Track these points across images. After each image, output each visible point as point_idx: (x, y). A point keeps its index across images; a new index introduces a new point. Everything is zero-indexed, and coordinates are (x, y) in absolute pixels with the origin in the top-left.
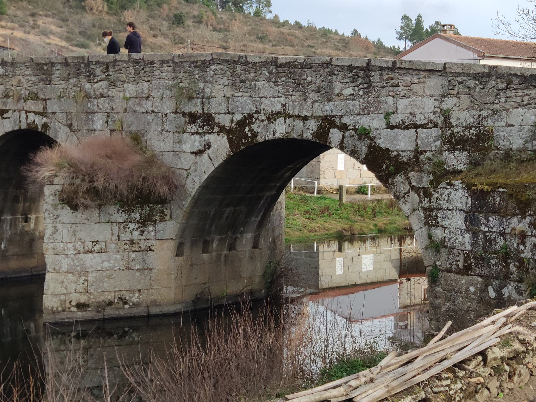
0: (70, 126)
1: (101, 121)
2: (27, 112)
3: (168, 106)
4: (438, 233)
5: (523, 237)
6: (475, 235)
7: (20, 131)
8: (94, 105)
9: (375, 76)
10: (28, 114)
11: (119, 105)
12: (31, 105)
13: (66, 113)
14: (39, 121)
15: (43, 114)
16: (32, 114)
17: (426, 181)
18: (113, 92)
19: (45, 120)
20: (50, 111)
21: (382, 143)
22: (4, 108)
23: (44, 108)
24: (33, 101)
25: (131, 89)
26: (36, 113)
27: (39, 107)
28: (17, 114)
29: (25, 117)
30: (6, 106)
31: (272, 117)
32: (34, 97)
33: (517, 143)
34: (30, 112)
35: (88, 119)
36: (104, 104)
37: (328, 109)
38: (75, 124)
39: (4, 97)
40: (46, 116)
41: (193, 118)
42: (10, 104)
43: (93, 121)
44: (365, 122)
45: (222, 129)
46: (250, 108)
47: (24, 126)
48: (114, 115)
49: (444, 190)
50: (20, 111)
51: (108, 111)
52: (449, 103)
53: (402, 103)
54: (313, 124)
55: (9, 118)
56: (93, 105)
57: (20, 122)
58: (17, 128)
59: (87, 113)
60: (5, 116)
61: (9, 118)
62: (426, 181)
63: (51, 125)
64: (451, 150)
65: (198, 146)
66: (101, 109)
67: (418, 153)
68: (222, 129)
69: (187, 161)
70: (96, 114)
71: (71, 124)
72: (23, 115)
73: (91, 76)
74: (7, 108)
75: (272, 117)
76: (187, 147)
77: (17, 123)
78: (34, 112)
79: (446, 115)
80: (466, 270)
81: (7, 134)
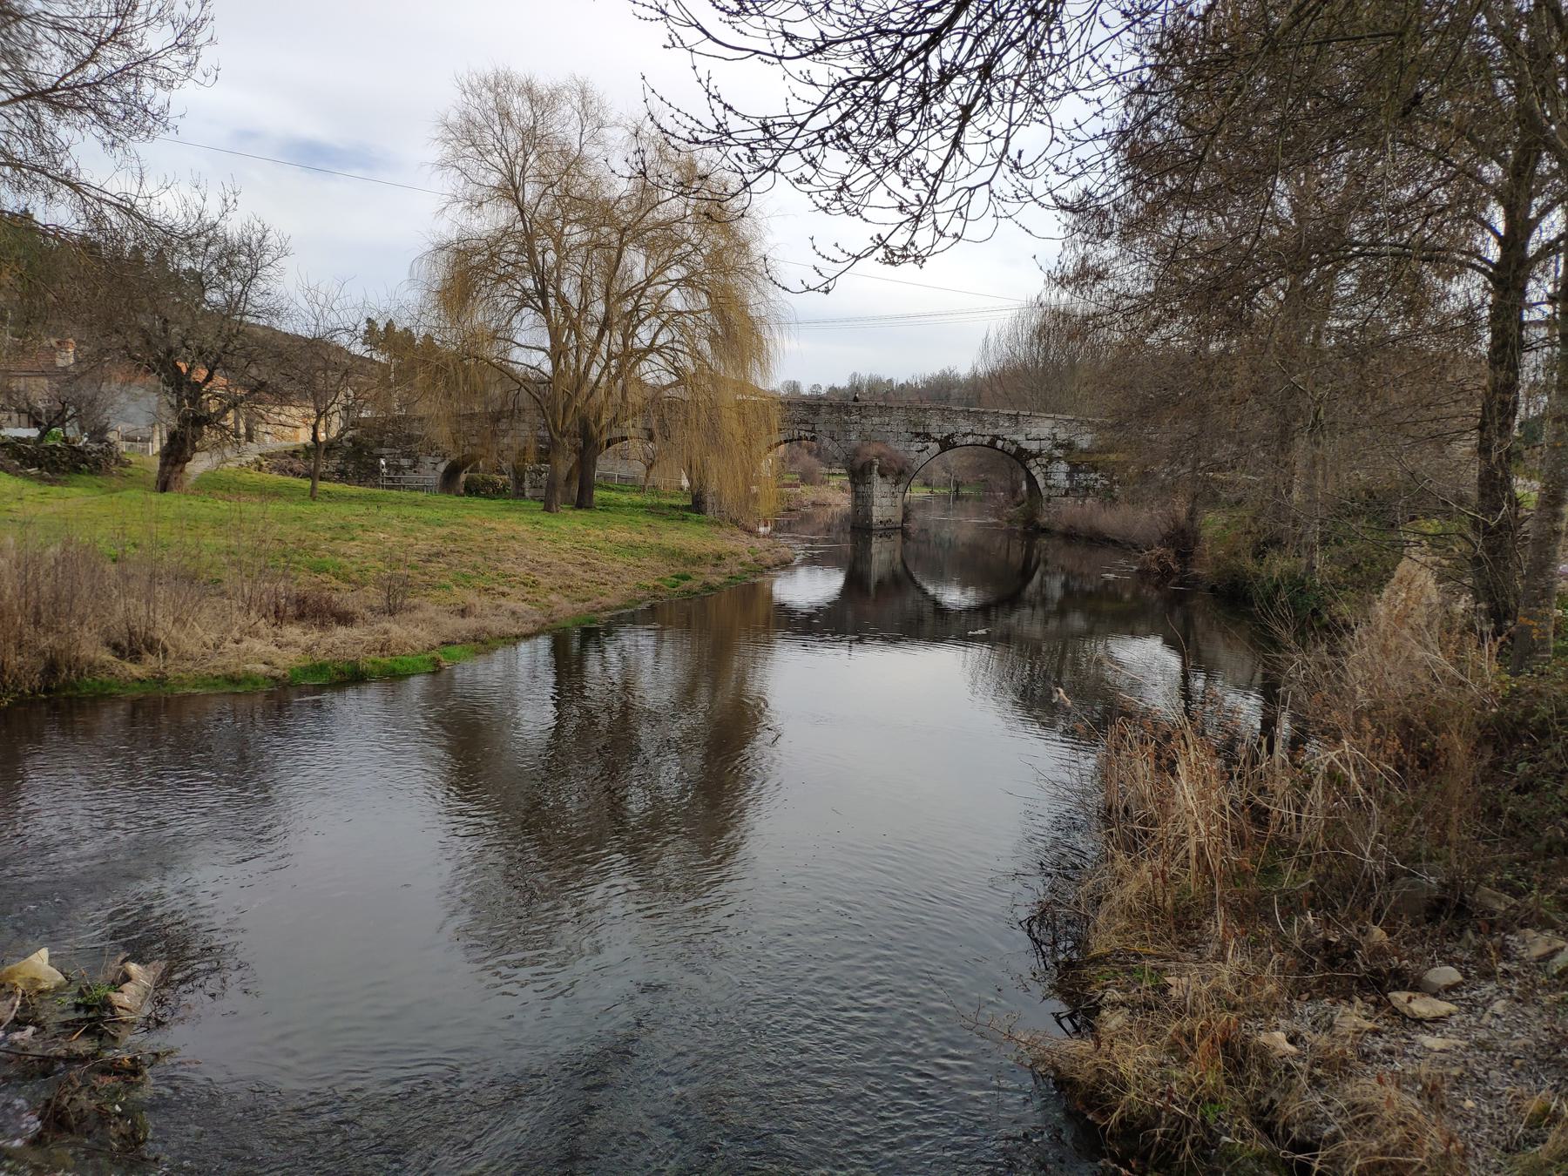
3: (902, 429)
4: (1051, 482)
5: (1096, 480)
6: (1072, 481)
9: (1021, 418)
11: (868, 428)
17: (1044, 461)
18: (863, 421)
21: (1023, 446)
25: (876, 420)
31: (965, 435)
33: (1086, 446)
37: (996, 432)
41: (918, 435)
44: (1015, 437)
45: (936, 440)
46: (952, 430)
49: (1055, 465)
52: (1056, 430)
53: (1034, 430)
54: (988, 439)
62: (1044, 461)
64: (1057, 448)
65: (920, 448)
67: (1041, 450)
68: (936, 440)
69: (914, 455)
73: (849, 413)
75: (965, 435)
76: (914, 449)
79: (1054, 435)
80: (1067, 494)
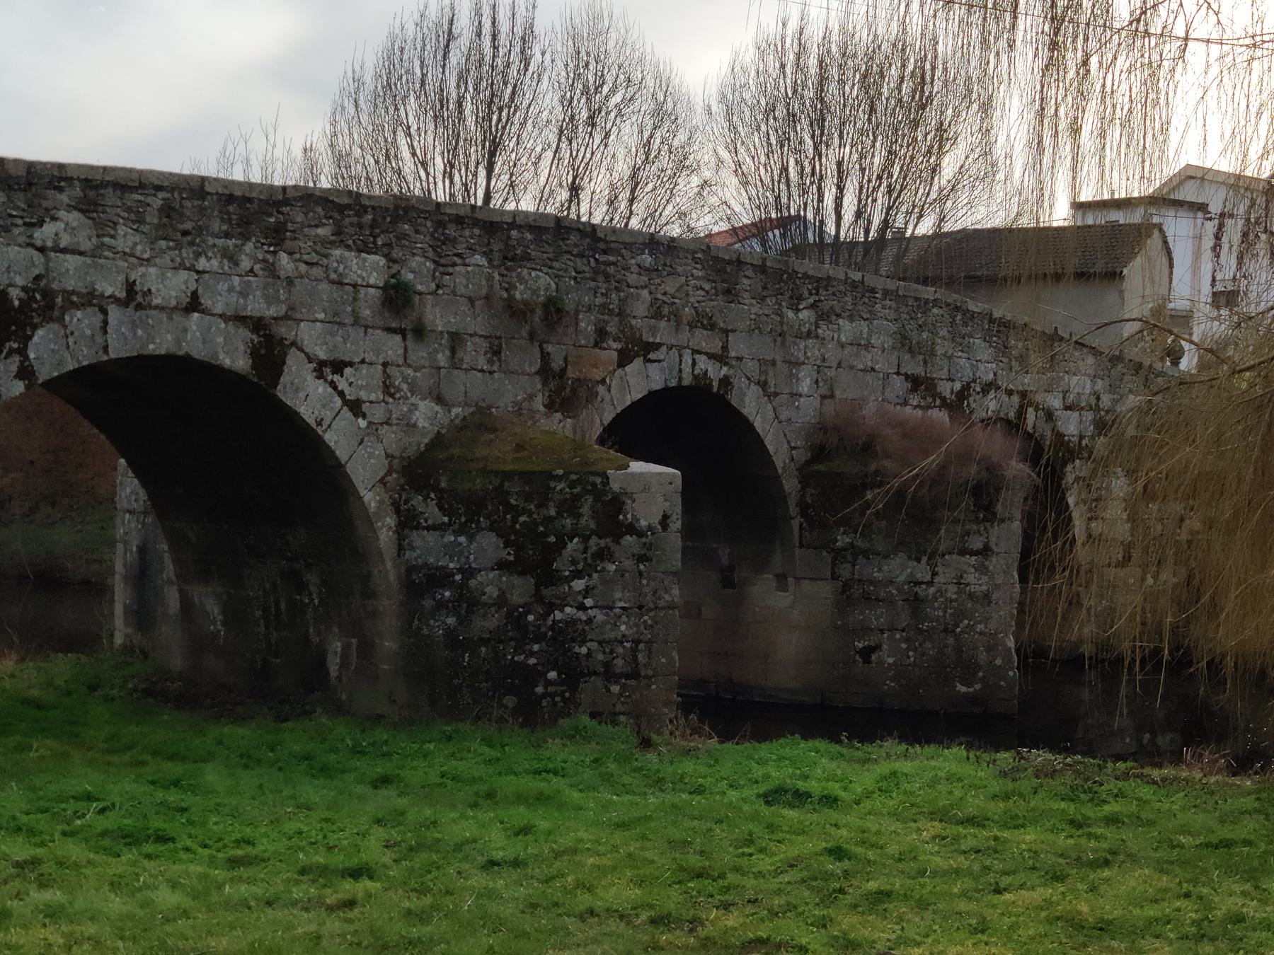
0: (763, 385)
1: (808, 380)
2: (695, 352)
7: (680, 388)
8: (799, 350)
10: (697, 357)
12: (702, 339)
13: (759, 360)
14: (716, 373)
15: (721, 358)
16: (704, 358)
19: (725, 370)
20: (733, 354)
22: (651, 340)
23: (722, 347)
24: (705, 332)
26: (711, 356)
27: (715, 346)
28: (674, 353)
29: (690, 361)
30: (654, 335)
32: (704, 322)
34: (699, 352)
35: (791, 375)
36: (812, 349)
38: (772, 382)
39: (652, 318)
40: (726, 364)
42: (663, 333)
43: (798, 379)
47: (687, 380)
48: (826, 370)
50: (680, 349)
51: (818, 362)
55: (659, 361)
56: (800, 349)
57: (680, 371)
58: (673, 383)
59: (790, 362)
60: (652, 356)
61: (659, 361)
63: (735, 381)
66: (808, 358)
70: (803, 367)
71: (766, 382)
72: (688, 359)
74: (658, 340)
77: (675, 373)
78: (706, 354)
81: (652, 394)
